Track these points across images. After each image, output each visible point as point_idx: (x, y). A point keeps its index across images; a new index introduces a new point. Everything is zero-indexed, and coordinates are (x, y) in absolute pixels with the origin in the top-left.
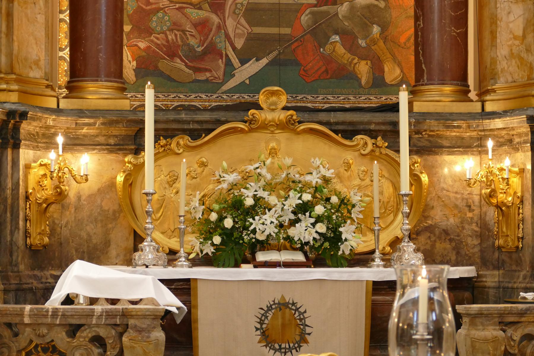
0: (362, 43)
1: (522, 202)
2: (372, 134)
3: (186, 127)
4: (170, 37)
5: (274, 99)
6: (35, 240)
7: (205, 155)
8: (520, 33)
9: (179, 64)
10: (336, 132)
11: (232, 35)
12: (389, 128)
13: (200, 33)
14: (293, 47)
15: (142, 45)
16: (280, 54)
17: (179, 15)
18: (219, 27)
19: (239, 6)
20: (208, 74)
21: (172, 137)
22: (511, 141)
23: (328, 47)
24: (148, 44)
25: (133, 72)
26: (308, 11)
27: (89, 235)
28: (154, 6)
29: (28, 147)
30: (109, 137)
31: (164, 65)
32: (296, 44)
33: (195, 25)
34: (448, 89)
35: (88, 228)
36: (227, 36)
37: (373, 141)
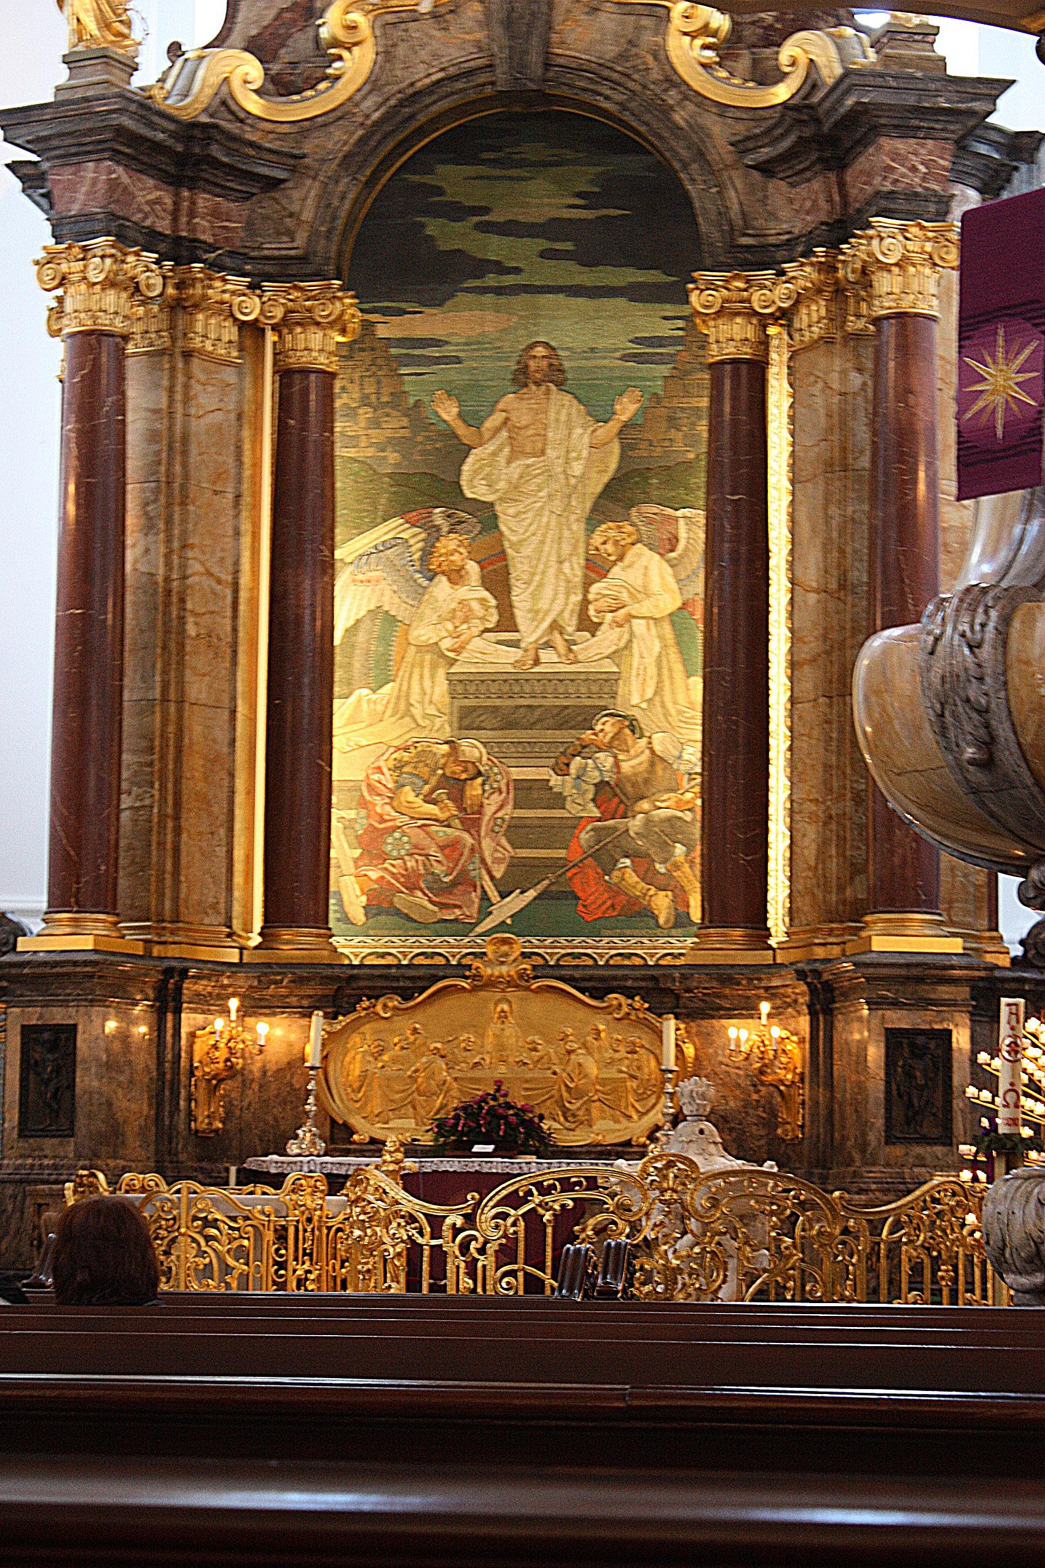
0: (661, 868)
1: (802, 1080)
2: (629, 994)
3: (394, 984)
4: (409, 864)
5: (505, 948)
6: (201, 1123)
7: (417, 1021)
8: (812, 863)
9: (420, 898)
10: (582, 991)
11: (489, 860)
12: (650, 985)
13: (447, 857)
14: (569, 874)
15: (374, 875)
16: (552, 884)
17: (422, 834)
18: (473, 850)
19: (499, 822)
20: (458, 912)
21: (377, 998)
22: (796, 1001)
23: (616, 873)
24: (381, 873)
25: (362, 911)
26: (589, 827)
27: (276, 1119)
28: (390, 824)
29: (194, 1011)
30: (302, 997)
31: (401, 901)
32: (574, 871)
33: (442, 848)
34: (737, 933)
35: (275, 1111)
36: (483, 861)
37: (630, 1001)
